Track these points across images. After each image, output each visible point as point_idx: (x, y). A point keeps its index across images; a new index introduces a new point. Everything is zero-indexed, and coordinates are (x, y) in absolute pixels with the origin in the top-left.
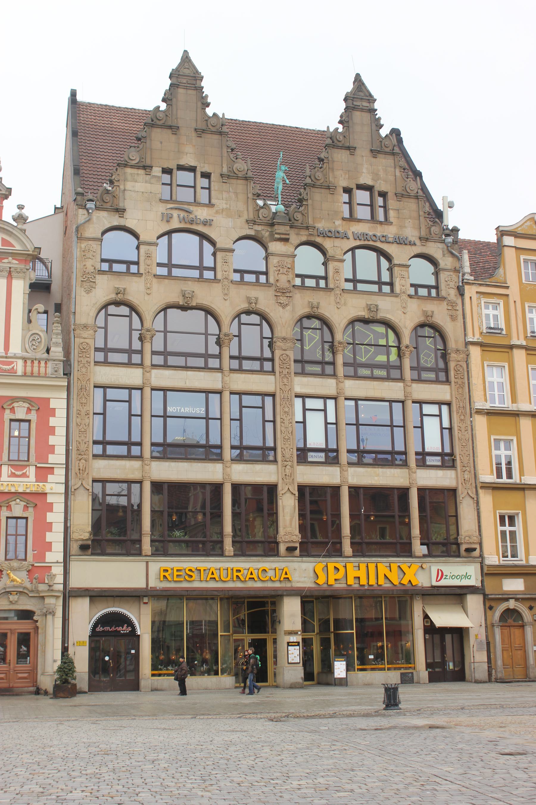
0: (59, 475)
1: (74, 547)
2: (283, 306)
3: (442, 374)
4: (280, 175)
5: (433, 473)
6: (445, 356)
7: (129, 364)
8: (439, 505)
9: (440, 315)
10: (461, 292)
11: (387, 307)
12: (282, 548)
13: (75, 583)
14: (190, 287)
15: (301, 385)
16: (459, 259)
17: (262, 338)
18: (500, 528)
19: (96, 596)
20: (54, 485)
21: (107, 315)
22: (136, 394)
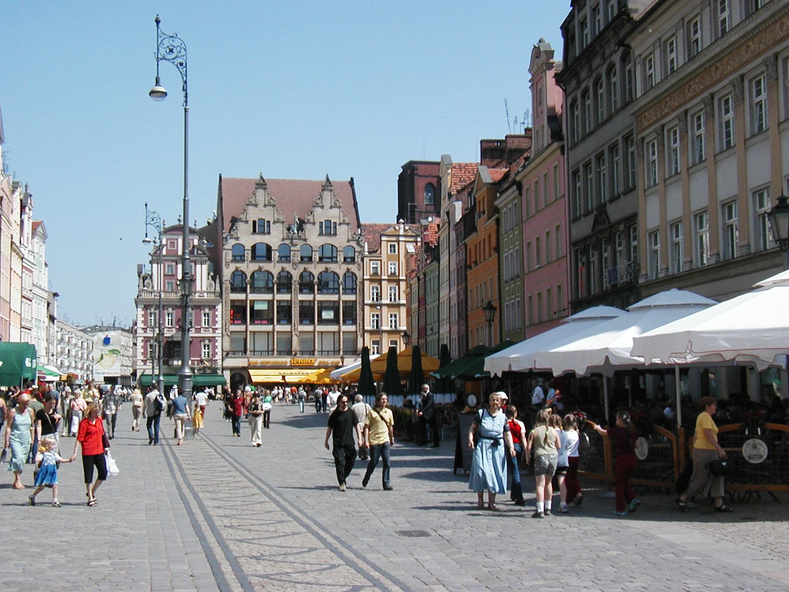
0: (219, 331)
2: (295, 269)
9: (353, 268)
10: (362, 260)
11: (333, 267)
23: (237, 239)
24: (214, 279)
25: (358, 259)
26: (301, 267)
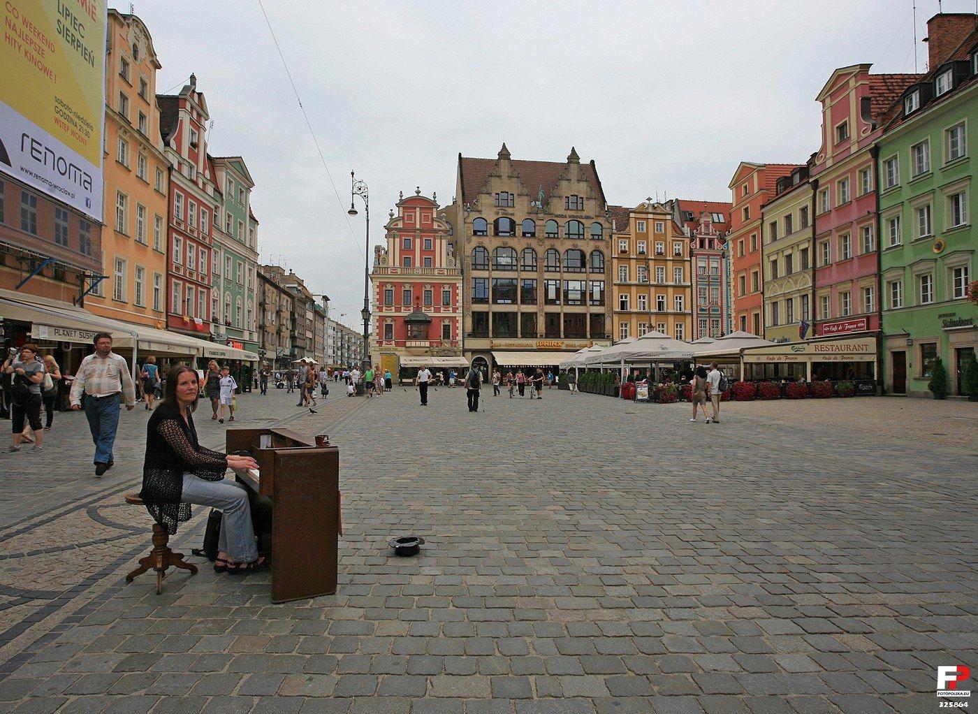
1: (466, 335)
2: (541, 246)
3: (601, 270)
4: (541, 193)
5: (595, 308)
6: (603, 262)
7: (484, 270)
8: (598, 319)
9: (602, 246)
11: (581, 244)
12: (538, 335)
13: (466, 347)
14: (506, 239)
15: (547, 275)
16: (612, 224)
17: (533, 258)
18: (621, 328)
19: (474, 352)
20: (459, 315)
21: (476, 251)
22: (486, 280)
23: (480, 212)
24: (454, 255)
25: (606, 237)
26: (548, 244)
